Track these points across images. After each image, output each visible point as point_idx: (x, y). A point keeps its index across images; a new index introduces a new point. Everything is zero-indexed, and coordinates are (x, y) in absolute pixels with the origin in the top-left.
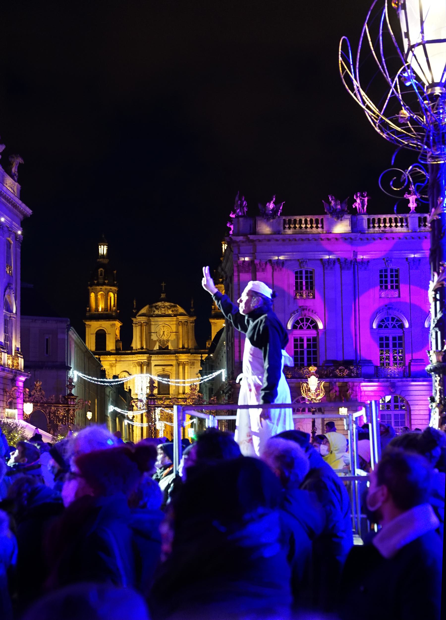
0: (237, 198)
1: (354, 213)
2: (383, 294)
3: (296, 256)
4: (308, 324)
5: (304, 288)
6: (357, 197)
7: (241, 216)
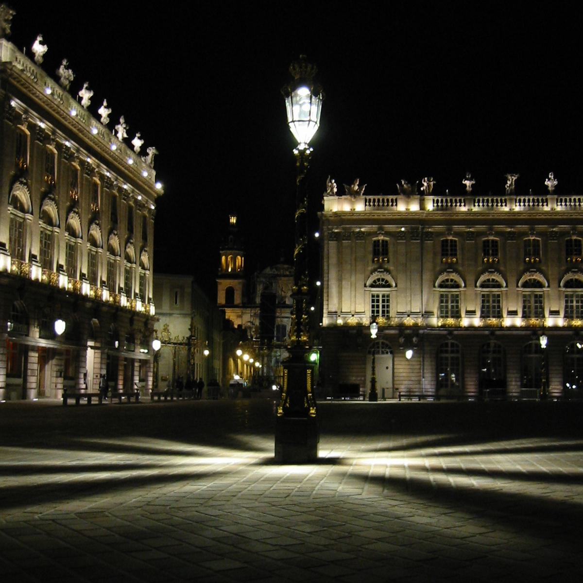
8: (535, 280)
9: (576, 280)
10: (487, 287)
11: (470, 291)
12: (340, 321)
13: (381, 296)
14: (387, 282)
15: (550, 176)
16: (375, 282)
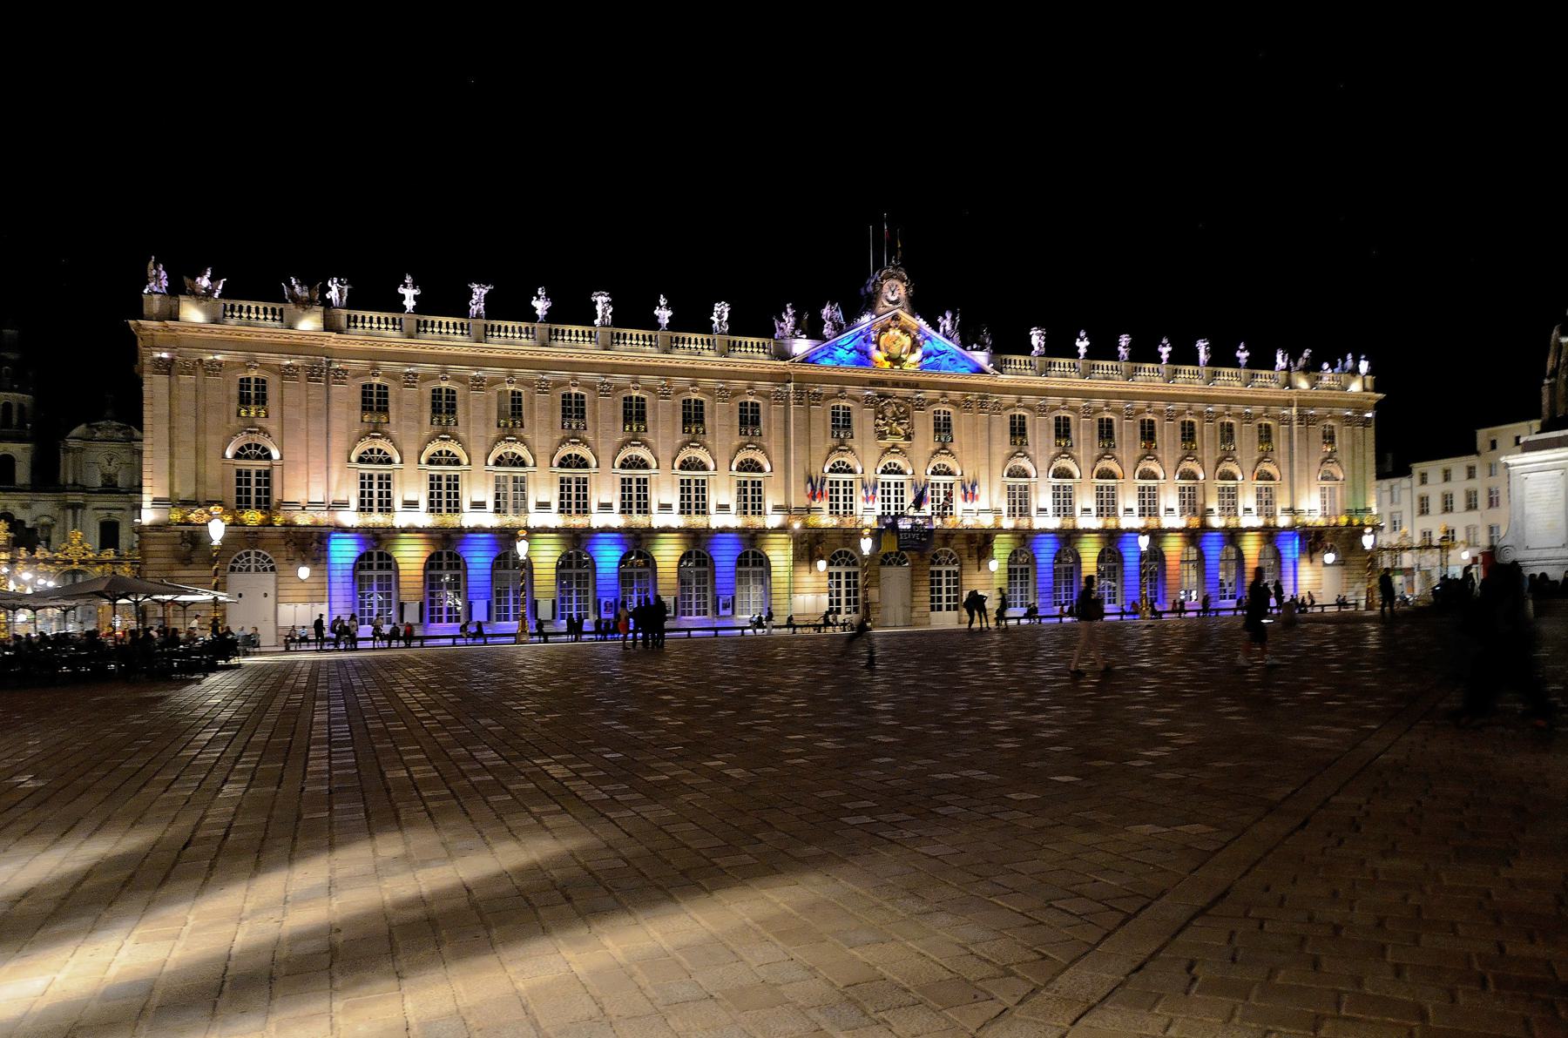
0: (151, 265)
1: (327, 304)
2: (366, 418)
5: (253, 401)
6: (332, 284)
7: (156, 293)
8: (514, 454)
9: (577, 456)
10: (439, 463)
11: (410, 468)
13: (253, 474)
14: (264, 450)
15: (539, 293)
16: (242, 449)
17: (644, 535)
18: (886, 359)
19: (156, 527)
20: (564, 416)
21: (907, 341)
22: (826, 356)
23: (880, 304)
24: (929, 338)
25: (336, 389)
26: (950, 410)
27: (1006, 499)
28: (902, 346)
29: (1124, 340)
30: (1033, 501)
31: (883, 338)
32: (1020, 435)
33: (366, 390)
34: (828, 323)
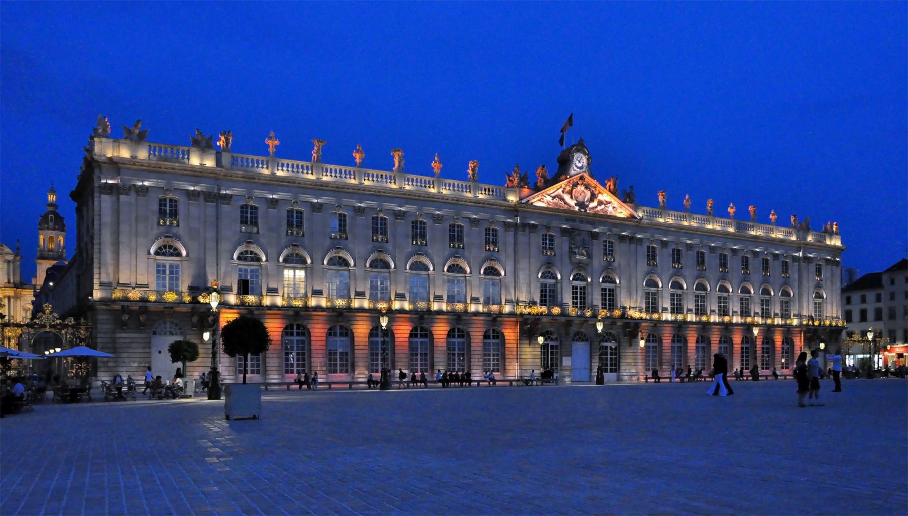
3: (161, 183)
4: (171, 251)
8: (340, 258)
12: (118, 294)
14: (175, 249)
16: (160, 248)
17: (426, 316)
18: (576, 205)
19: (102, 301)
20: (373, 233)
21: (588, 194)
22: (540, 200)
23: (571, 169)
24: (600, 193)
25: (225, 208)
26: (613, 240)
27: (644, 301)
28: (585, 197)
29: (710, 203)
30: (660, 303)
31: (574, 191)
32: (652, 259)
33: (244, 208)
34: (541, 178)
